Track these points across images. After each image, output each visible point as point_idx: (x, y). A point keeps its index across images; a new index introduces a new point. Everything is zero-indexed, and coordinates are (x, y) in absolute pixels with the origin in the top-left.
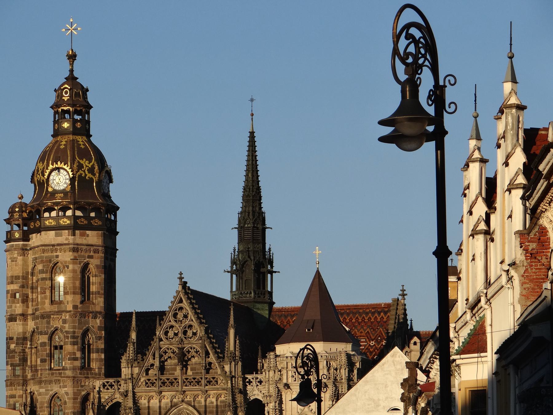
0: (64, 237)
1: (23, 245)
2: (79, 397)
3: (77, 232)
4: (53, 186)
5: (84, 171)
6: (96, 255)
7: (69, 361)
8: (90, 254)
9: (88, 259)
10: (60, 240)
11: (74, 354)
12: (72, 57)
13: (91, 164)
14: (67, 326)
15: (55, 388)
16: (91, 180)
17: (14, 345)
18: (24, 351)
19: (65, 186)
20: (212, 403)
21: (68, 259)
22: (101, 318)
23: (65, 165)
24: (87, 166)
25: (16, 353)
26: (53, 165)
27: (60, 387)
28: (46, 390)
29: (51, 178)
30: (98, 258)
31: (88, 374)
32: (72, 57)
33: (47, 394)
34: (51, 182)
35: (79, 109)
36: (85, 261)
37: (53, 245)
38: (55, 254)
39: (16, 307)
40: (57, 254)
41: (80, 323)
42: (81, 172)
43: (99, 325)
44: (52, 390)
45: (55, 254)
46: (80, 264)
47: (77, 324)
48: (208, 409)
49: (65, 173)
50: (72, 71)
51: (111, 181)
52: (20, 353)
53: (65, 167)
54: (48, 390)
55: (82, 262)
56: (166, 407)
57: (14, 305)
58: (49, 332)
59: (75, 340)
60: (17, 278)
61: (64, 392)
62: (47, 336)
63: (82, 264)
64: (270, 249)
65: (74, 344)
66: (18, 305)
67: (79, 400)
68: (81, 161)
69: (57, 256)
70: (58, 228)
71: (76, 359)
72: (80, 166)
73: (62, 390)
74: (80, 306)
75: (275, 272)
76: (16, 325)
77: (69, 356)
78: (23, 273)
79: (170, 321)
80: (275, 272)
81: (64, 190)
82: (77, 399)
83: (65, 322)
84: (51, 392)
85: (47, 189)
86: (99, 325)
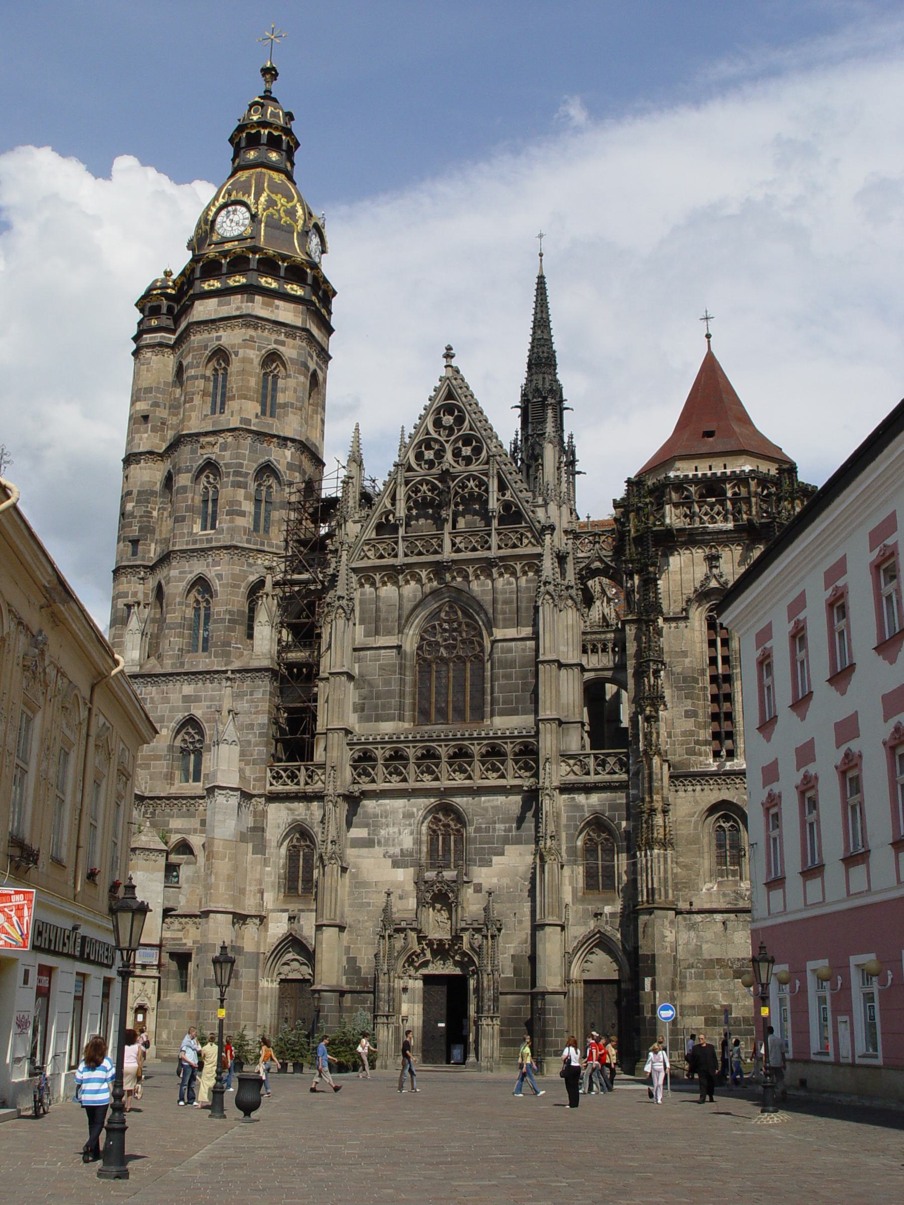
0: (234, 306)
1: (161, 337)
2: (243, 585)
3: (258, 298)
4: (221, 231)
5: (278, 211)
6: (289, 341)
7: (228, 517)
8: (279, 338)
9: (275, 346)
10: (225, 311)
11: (239, 503)
12: (270, 73)
13: (291, 204)
14: (227, 454)
15: (197, 567)
16: (289, 230)
17: (133, 504)
18: (148, 514)
19: (243, 229)
20: (510, 584)
21: (240, 341)
22: (293, 450)
23: (244, 195)
24: (283, 205)
25: (135, 517)
27: (208, 566)
28: (181, 573)
29: (219, 219)
30: (293, 347)
31: (263, 544)
33: (181, 580)
34: (217, 226)
35: (276, 133)
36: (270, 347)
37: (213, 321)
38: (215, 335)
39: (141, 439)
40: (219, 334)
41: (253, 450)
43: (289, 459)
44: (191, 572)
45: (215, 335)
46: (259, 349)
47: (247, 452)
48: (500, 597)
49: (244, 209)
51: (323, 251)
52: (141, 517)
53: (245, 199)
54: (185, 572)
55: (264, 348)
56: (415, 596)
57: (137, 436)
58: (195, 465)
59: (241, 479)
60: (149, 390)
61: (213, 574)
62: (190, 475)
63: (263, 352)
64: (571, 437)
65: (238, 485)
66: (146, 435)
67: (242, 589)
68: (273, 196)
69: (219, 338)
71: (242, 514)
73: (210, 571)
74: (254, 421)
75: (579, 473)
76: (138, 471)
77: (227, 508)
78: (159, 383)
79: (428, 433)
80: (579, 473)
81: (241, 235)
82: (239, 587)
83: (224, 448)
84: (189, 576)
86: (289, 459)
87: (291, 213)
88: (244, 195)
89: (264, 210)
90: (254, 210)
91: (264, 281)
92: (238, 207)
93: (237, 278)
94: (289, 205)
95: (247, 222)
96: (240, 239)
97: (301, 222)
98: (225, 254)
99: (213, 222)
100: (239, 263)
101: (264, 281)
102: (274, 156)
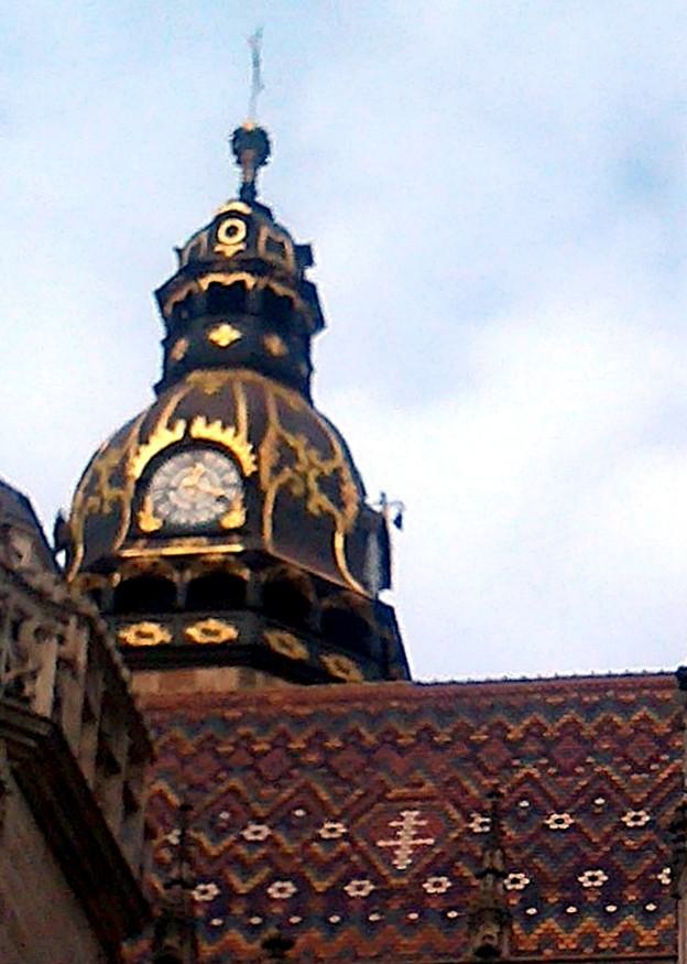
5: (305, 477)
16: (327, 524)
26: (170, 427)
35: (279, 289)
42: (287, 472)
49: (224, 463)
50: (248, 192)
53: (226, 437)
85: (135, 520)
87: (331, 485)
88: (224, 427)
89: (276, 470)
90: (249, 468)
91: (275, 639)
92: (209, 456)
93: (212, 624)
94: (328, 468)
96: (216, 532)
97: (352, 509)
98: (181, 562)
99: (143, 483)
101: (275, 639)
102: (275, 345)
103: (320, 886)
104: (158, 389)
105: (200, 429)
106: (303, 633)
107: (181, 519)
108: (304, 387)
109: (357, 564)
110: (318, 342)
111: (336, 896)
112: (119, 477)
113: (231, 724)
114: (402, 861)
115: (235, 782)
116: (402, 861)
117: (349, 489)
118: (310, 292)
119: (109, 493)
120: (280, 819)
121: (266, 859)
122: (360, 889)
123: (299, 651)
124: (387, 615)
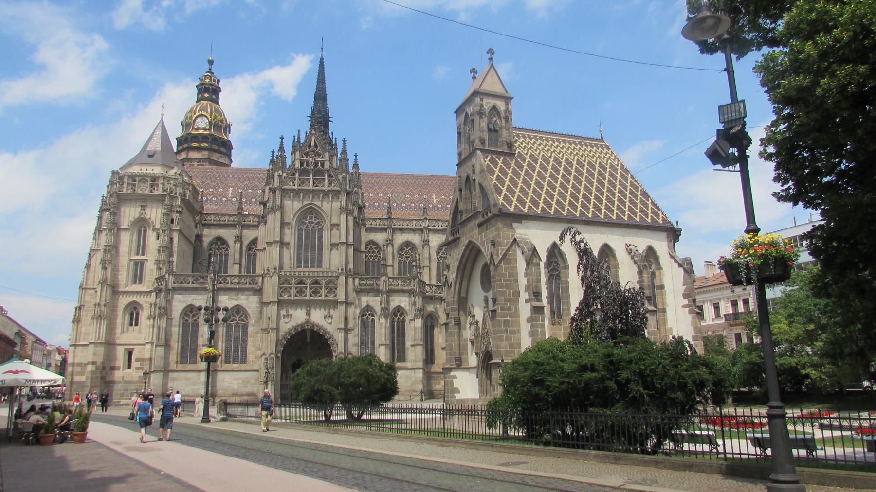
12: (211, 62)
16: (221, 127)
29: (197, 120)
32: (211, 62)
34: (196, 123)
35: (215, 88)
49: (206, 119)
50: (210, 69)
51: (230, 133)
53: (207, 115)
70: (199, 149)
72: (215, 117)
85: (193, 126)
87: (222, 121)
89: (214, 119)
95: (207, 123)
96: (205, 129)
99: (195, 121)
100: (204, 138)
102: (214, 97)
103: (219, 199)
104: (197, 102)
105: (203, 113)
106: (218, 145)
107: (200, 127)
108: (218, 103)
109: (225, 133)
110: (220, 93)
111: (221, 200)
112: (191, 118)
113: (208, 172)
114: (230, 196)
115: (208, 181)
116: (230, 196)
117: (224, 121)
118: (219, 88)
119: (190, 120)
120: (214, 188)
121: (212, 194)
122: (224, 199)
123: (217, 148)
124: (229, 141)
